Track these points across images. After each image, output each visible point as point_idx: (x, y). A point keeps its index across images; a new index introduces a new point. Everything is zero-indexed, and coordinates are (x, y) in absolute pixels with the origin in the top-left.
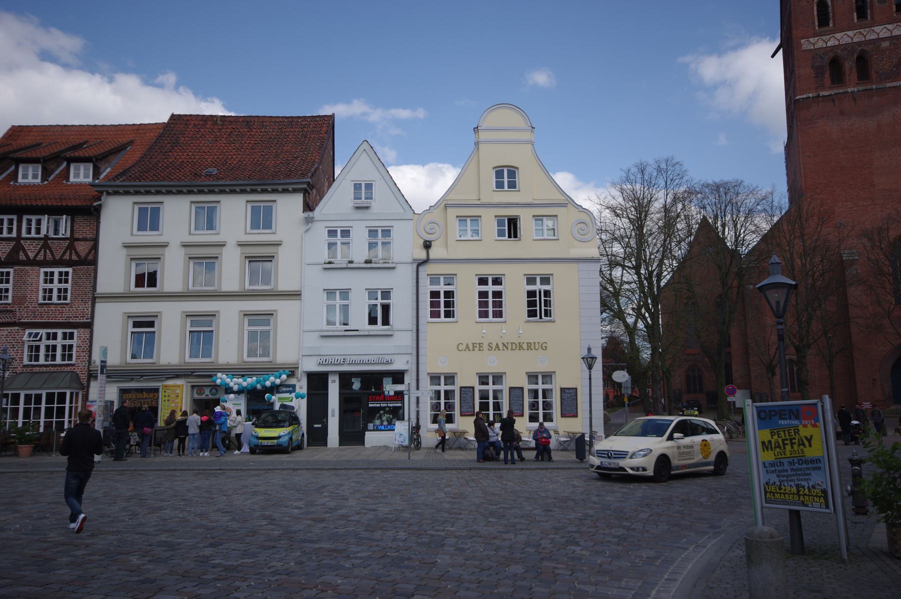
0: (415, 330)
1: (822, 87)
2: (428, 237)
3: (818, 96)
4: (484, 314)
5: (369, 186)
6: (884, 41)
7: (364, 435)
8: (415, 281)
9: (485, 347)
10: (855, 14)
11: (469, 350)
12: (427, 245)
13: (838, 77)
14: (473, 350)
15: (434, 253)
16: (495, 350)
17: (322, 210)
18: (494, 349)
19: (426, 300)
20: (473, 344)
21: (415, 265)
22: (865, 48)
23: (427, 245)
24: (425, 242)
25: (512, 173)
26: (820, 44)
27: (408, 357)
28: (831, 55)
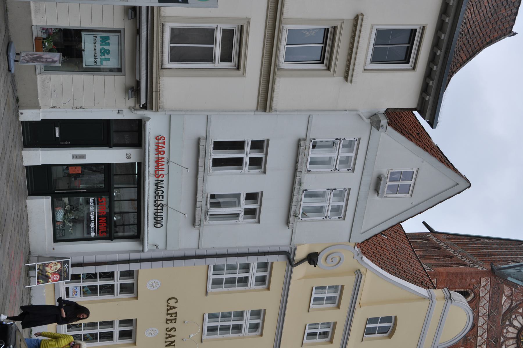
0: (200, 252)
2: (321, 259)
7: (46, 194)
8: (266, 250)
9: (171, 325)
11: (168, 310)
14: (168, 314)
16: (166, 334)
18: (168, 333)
20: (176, 313)
21: (286, 249)
27: (161, 246)
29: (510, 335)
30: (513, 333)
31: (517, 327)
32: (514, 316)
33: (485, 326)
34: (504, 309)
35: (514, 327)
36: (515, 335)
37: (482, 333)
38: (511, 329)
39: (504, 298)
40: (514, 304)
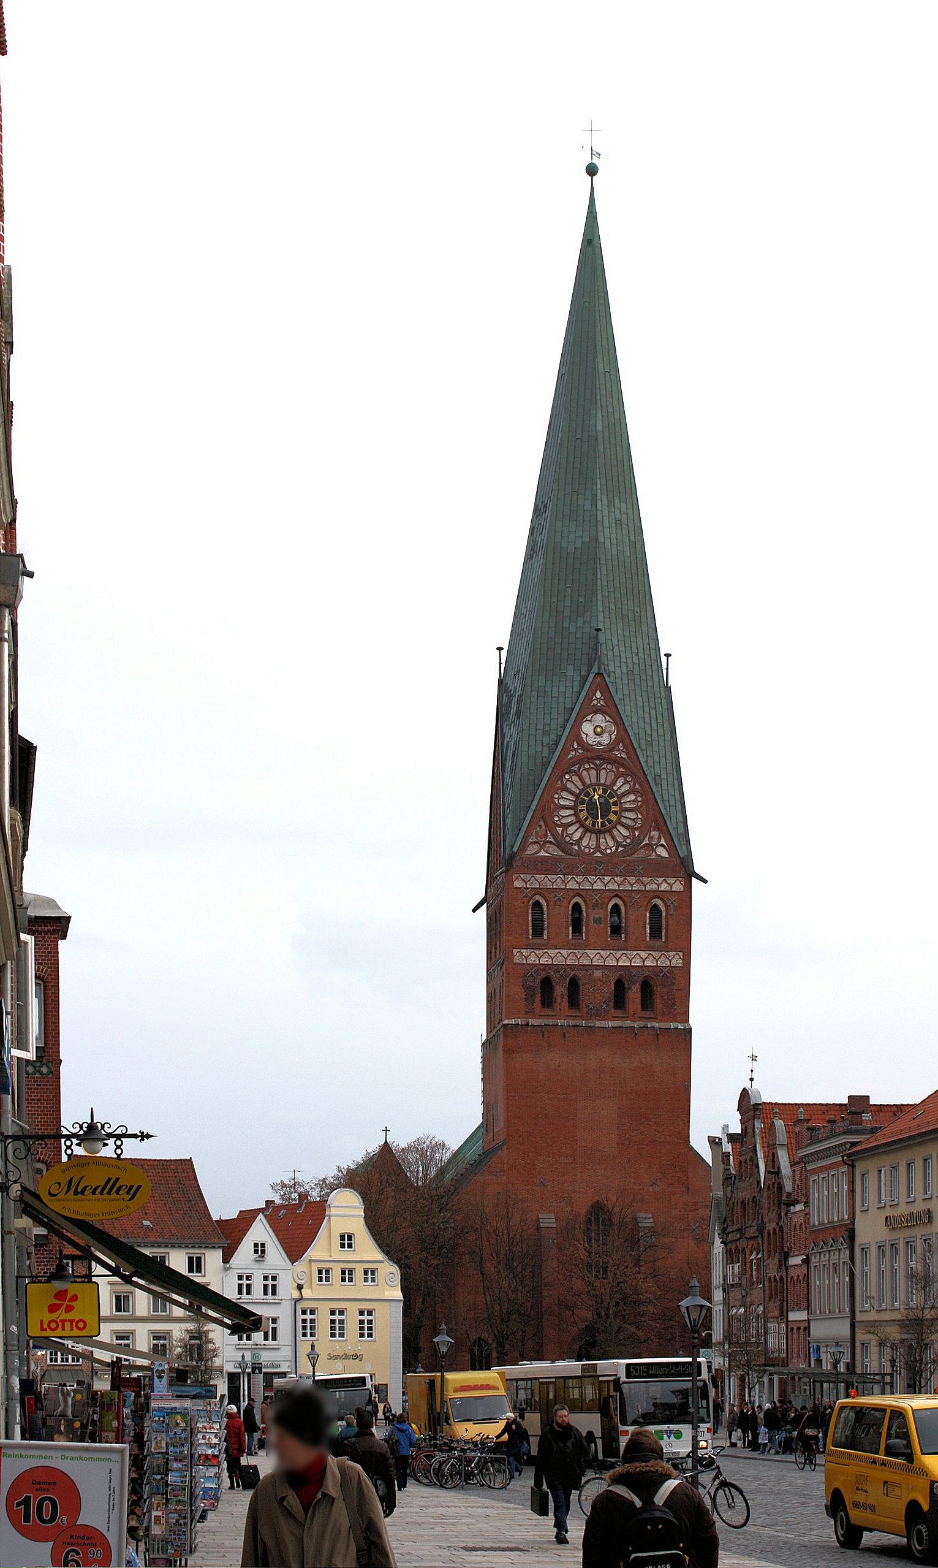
0: (294, 1345)
1: (531, 1013)
3: (528, 1025)
4: (333, 1335)
5: (263, 1245)
6: (596, 969)
8: (293, 1312)
10: (571, 928)
12: (300, 1287)
13: (548, 1000)
15: (306, 1293)
17: (234, 1261)
19: (300, 1324)
21: (293, 1302)
22: (577, 974)
23: (300, 1287)
24: (298, 1285)
25: (350, 1238)
26: (532, 959)
27: (289, 1363)
28: (543, 975)
29: (593, 843)
30: (590, 839)
31: (582, 833)
32: (568, 839)
33: (579, 879)
34: (557, 852)
35: (581, 838)
36: (594, 836)
37: (588, 883)
38: (584, 843)
39: (543, 854)
40: (552, 840)
